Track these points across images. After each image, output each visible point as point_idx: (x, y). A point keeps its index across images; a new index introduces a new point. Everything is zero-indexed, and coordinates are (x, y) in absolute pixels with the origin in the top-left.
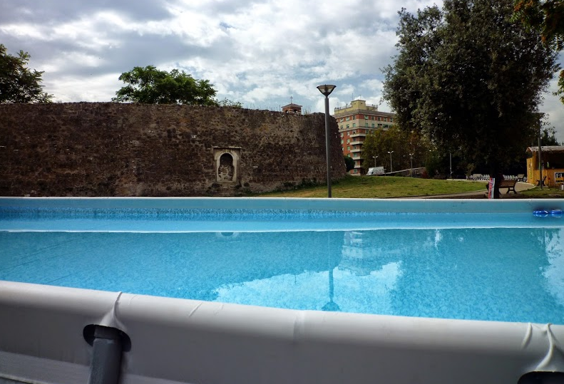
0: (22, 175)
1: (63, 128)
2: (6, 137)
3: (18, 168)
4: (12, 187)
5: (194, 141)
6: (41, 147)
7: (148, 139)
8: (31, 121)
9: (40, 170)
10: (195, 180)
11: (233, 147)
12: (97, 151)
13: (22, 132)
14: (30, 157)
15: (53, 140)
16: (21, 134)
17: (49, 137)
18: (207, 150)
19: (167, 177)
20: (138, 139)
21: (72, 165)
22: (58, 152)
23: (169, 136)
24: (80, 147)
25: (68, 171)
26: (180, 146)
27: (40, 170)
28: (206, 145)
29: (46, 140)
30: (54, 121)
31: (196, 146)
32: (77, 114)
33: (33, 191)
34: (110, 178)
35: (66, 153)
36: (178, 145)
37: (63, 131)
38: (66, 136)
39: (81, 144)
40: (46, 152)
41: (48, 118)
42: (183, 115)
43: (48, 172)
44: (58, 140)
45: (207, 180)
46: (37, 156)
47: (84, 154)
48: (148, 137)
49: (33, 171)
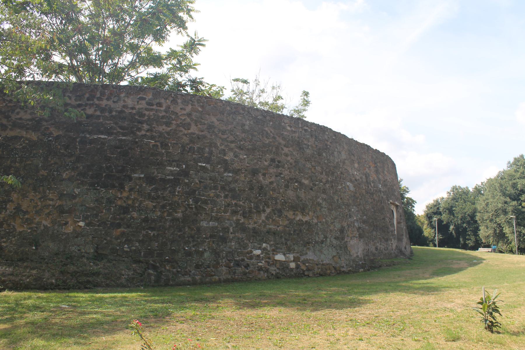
0: (244, 217)
1: (286, 150)
2: (207, 149)
3: (236, 205)
4: (231, 236)
5: (380, 191)
6: (264, 175)
7: (356, 183)
8: (244, 131)
9: (268, 210)
10: (387, 240)
11: (397, 203)
12: (324, 191)
13: (233, 145)
14: (251, 189)
15: (278, 167)
16: (231, 150)
17: (273, 160)
18: (388, 204)
19: (374, 233)
20: (351, 181)
21: (303, 210)
22: (287, 186)
23: (367, 181)
24: (306, 182)
25: (299, 217)
26: (374, 196)
27: (268, 210)
28: (387, 198)
29: (270, 165)
30: (274, 138)
31: (382, 197)
32: (297, 135)
33: (264, 245)
34: (342, 230)
35: (296, 189)
36: (372, 194)
37: (287, 155)
38: (291, 164)
39: (308, 179)
40: (271, 183)
41: (267, 133)
42: (370, 157)
43: (280, 216)
44: (283, 167)
45: (393, 240)
46: (261, 188)
47: (313, 193)
48: (356, 180)
49: (259, 212)
